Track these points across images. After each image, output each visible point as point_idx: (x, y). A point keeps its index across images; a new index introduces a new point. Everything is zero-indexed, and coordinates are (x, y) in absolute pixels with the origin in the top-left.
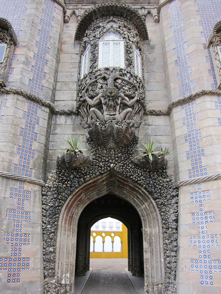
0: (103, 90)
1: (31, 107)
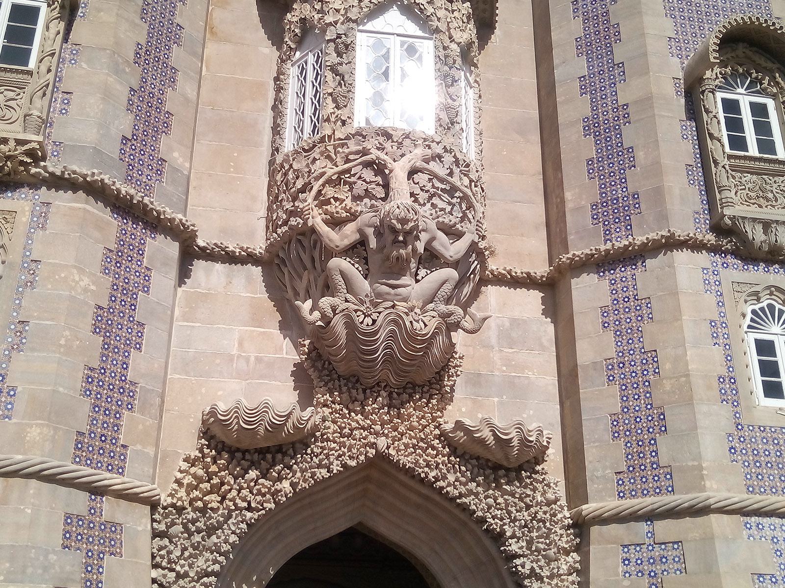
0: (372, 206)
1: (126, 233)
